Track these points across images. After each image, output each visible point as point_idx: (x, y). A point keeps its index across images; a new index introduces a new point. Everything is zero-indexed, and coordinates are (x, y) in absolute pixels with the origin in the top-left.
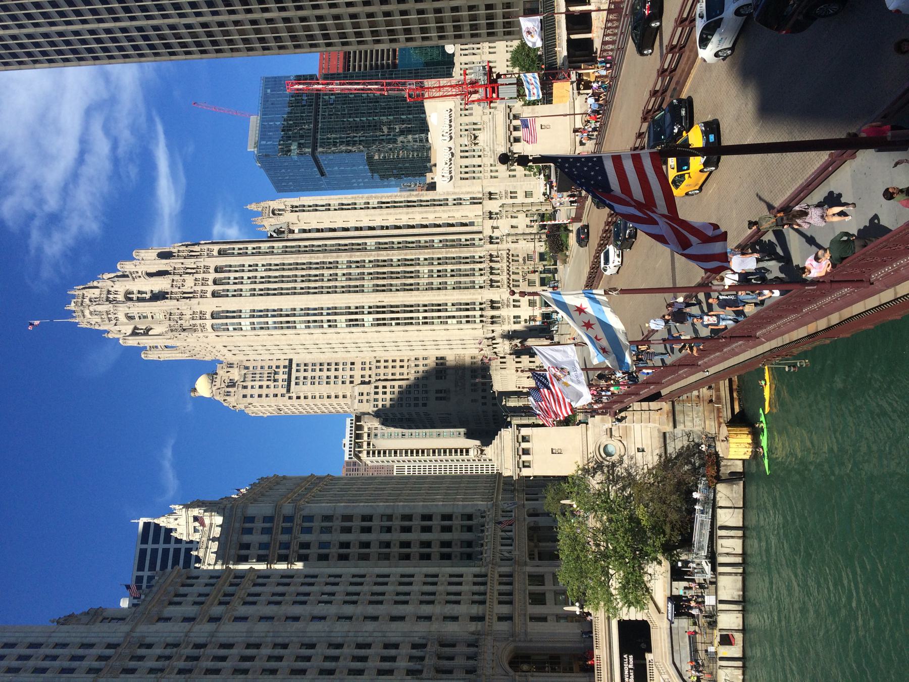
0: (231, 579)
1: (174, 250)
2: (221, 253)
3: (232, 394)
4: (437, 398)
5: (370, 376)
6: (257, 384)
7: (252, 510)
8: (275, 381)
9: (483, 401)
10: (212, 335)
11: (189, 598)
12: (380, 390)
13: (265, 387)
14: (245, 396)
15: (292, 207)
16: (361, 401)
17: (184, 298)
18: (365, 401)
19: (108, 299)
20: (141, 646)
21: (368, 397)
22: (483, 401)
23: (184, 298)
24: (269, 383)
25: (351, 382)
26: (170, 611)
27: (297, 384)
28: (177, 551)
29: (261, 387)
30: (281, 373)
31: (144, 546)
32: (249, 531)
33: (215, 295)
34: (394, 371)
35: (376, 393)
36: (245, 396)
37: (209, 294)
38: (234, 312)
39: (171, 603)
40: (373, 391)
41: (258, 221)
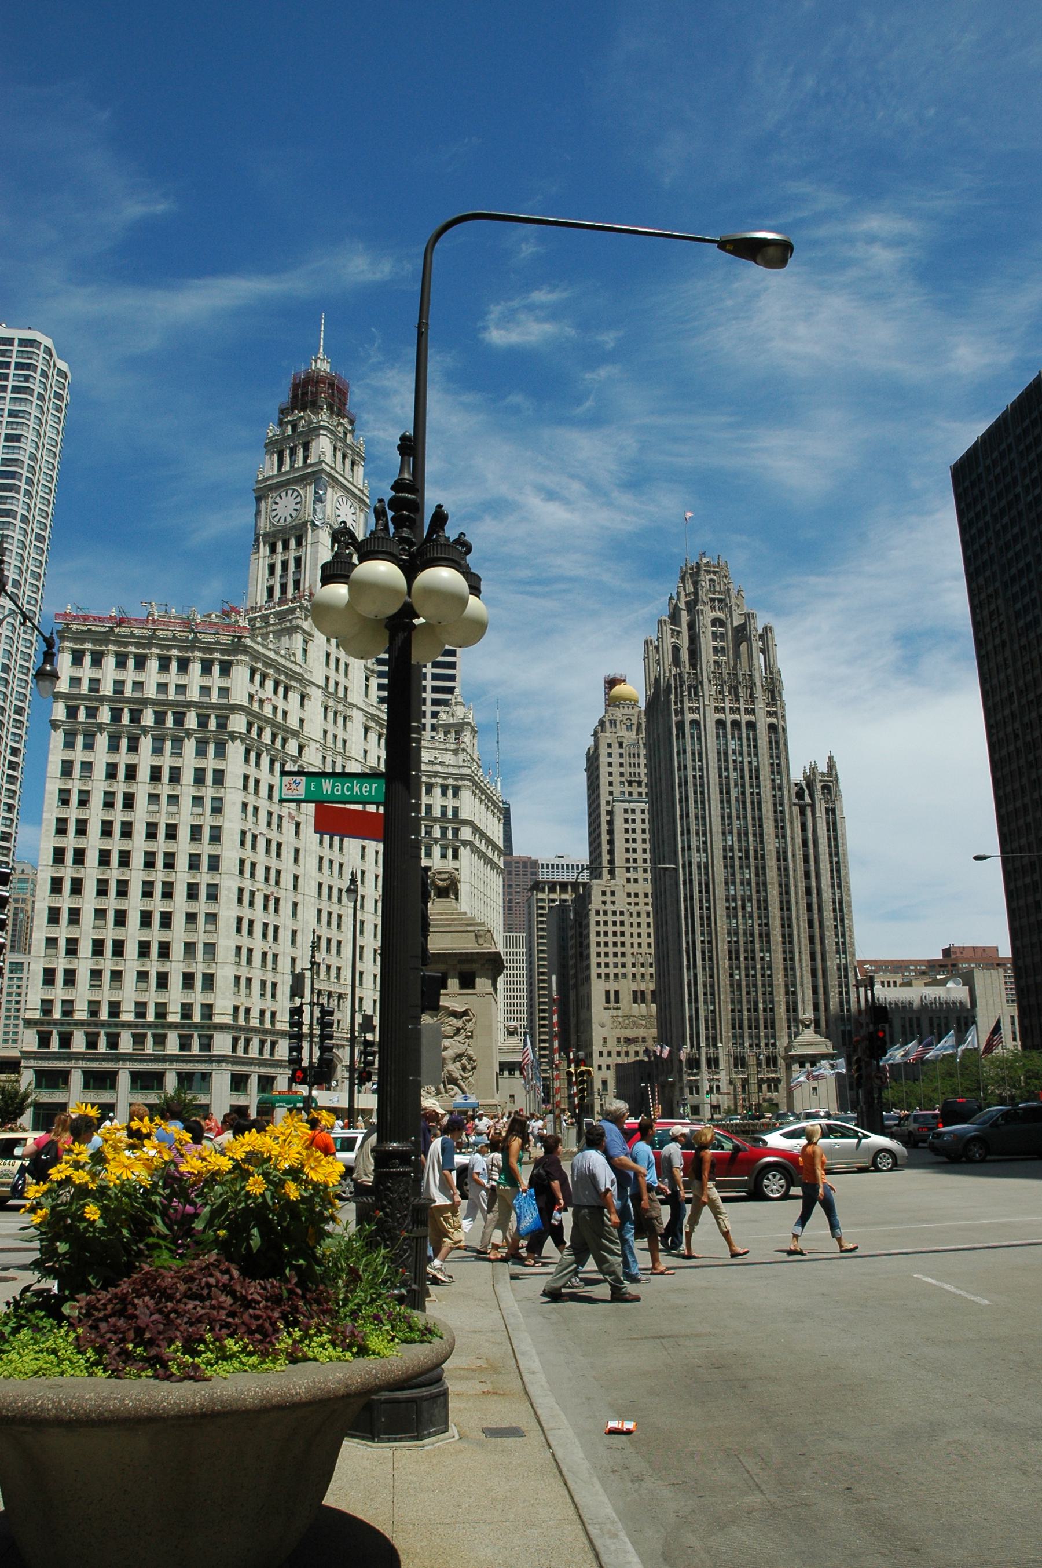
4: (607, 993)
5: (637, 904)
6: (625, 760)
7: (466, 795)
8: (630, 783)
9: (605, 1054)
12: (618, 918)
13: (622, 770)
14: (609, 746)
15: (833, 810)
16: (604, 893)
18: (604, 898)
19: (712, 600)
20: (345, 718)
21: (609, 902)
22: (605, 1054)
24: (627, 775)
25: (628, 880)
27: (626, 811)
29: (621, 765)
30: (640, 789)
32: (444, 794)
33: (720, 723)
34: (644, 935)
35: (614, 913)
36: (609, 746)
40: (617, 908)
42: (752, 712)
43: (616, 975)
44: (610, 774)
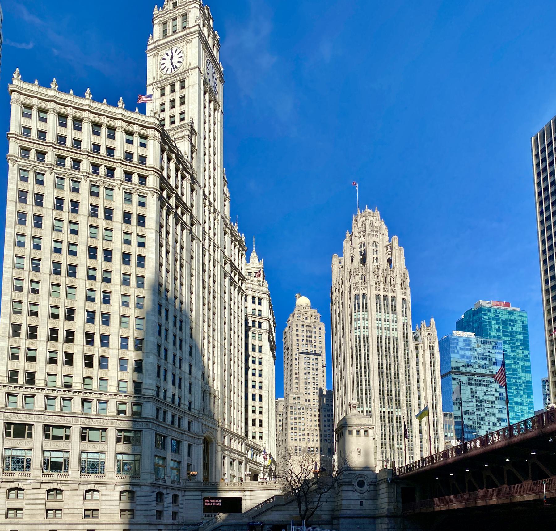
43: (300, 440)
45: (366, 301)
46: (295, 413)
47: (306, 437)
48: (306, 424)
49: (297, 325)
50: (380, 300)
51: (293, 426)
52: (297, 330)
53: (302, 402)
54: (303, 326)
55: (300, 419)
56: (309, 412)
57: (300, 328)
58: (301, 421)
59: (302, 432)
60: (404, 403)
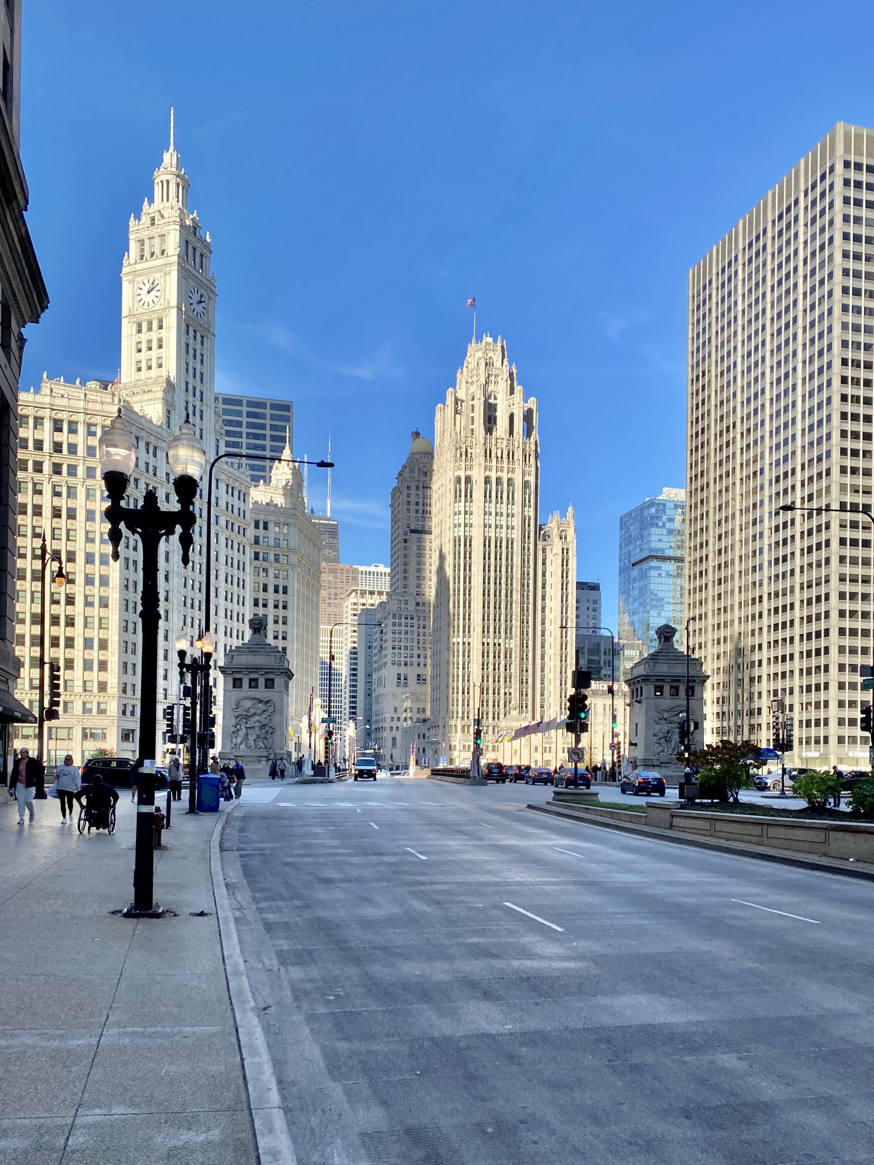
0: (243, 526)
1: (532, 438)
2: (526, 485)
3: (412, 475)
10: (451, 475)
11: (231, 498)
13: (417, 508)
17: (486, 450)
23: (486, 450)
24: (421, 511)
26: (222, 487)
28: (263, 468)
31: (268, 406)
37: (487, 473)
38: (471, 496)
39: (227, 486)
41: (557, 515)
42: (513, 472)
43: (406, 664)
44: (408, 510)
45: (472, 486)
46: (400, 625)
47: (415, 660)
48: (416, 641)
49: (409, 488)
50: (491, 486)
51: (396, 644)
52: (408, 496)
53: (412, 607)
54: (417, 488)
55: (406, 633)
56: (422, 623)
57: (413, 491)
58: (409, 636)
59: (408, 652)
60: (516, 632)
